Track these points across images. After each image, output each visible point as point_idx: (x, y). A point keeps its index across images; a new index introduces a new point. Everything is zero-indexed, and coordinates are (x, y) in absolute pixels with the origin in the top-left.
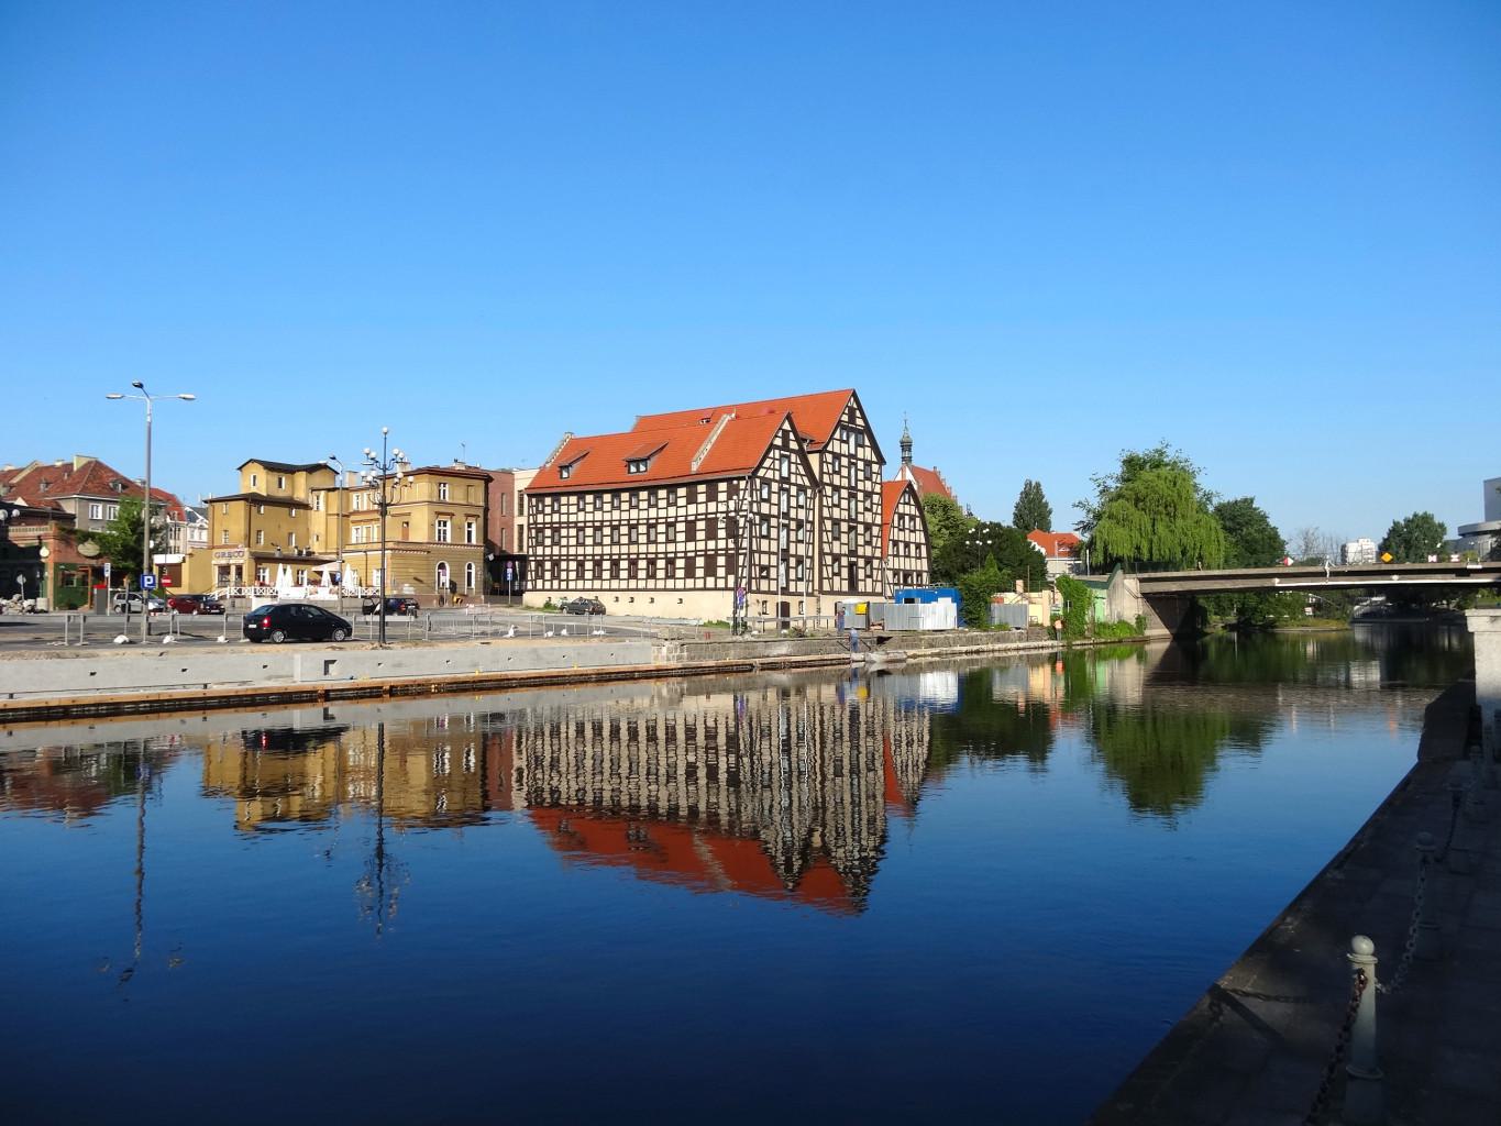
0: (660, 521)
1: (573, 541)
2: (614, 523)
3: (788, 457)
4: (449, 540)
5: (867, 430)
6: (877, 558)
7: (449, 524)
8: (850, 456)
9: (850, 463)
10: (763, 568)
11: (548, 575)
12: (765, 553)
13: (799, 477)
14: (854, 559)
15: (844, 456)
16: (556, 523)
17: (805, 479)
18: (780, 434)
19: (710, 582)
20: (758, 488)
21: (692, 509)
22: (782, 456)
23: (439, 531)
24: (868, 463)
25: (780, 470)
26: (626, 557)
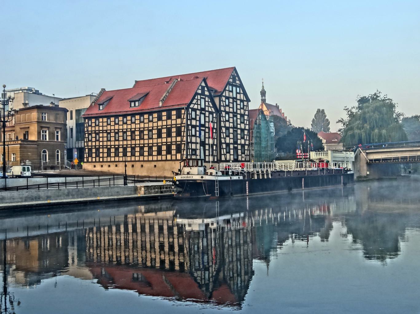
0: (145, 129)
1: (105, 139)
2: (124, 130)
3: (205, 99)
4: (47, 139)
5: (241, 86)
6: (247, 145)
7: (47, 132)
8: (233, 98)
9: (233, 101)
10: (193, 150)
11: (94, 155)
12: (194, 143)
13: (210, 108)
14: (236, 146)
15: (231, 98)
16: (97, 131)
17: (213, 109)
18: (200, 88)
19: (169, 157)
20: (190, 113)
21: (160, 123)
22: (201, 98)
23: (43, 135)
24: (242, 101)
25: (200, 105)
26: (130, 146)
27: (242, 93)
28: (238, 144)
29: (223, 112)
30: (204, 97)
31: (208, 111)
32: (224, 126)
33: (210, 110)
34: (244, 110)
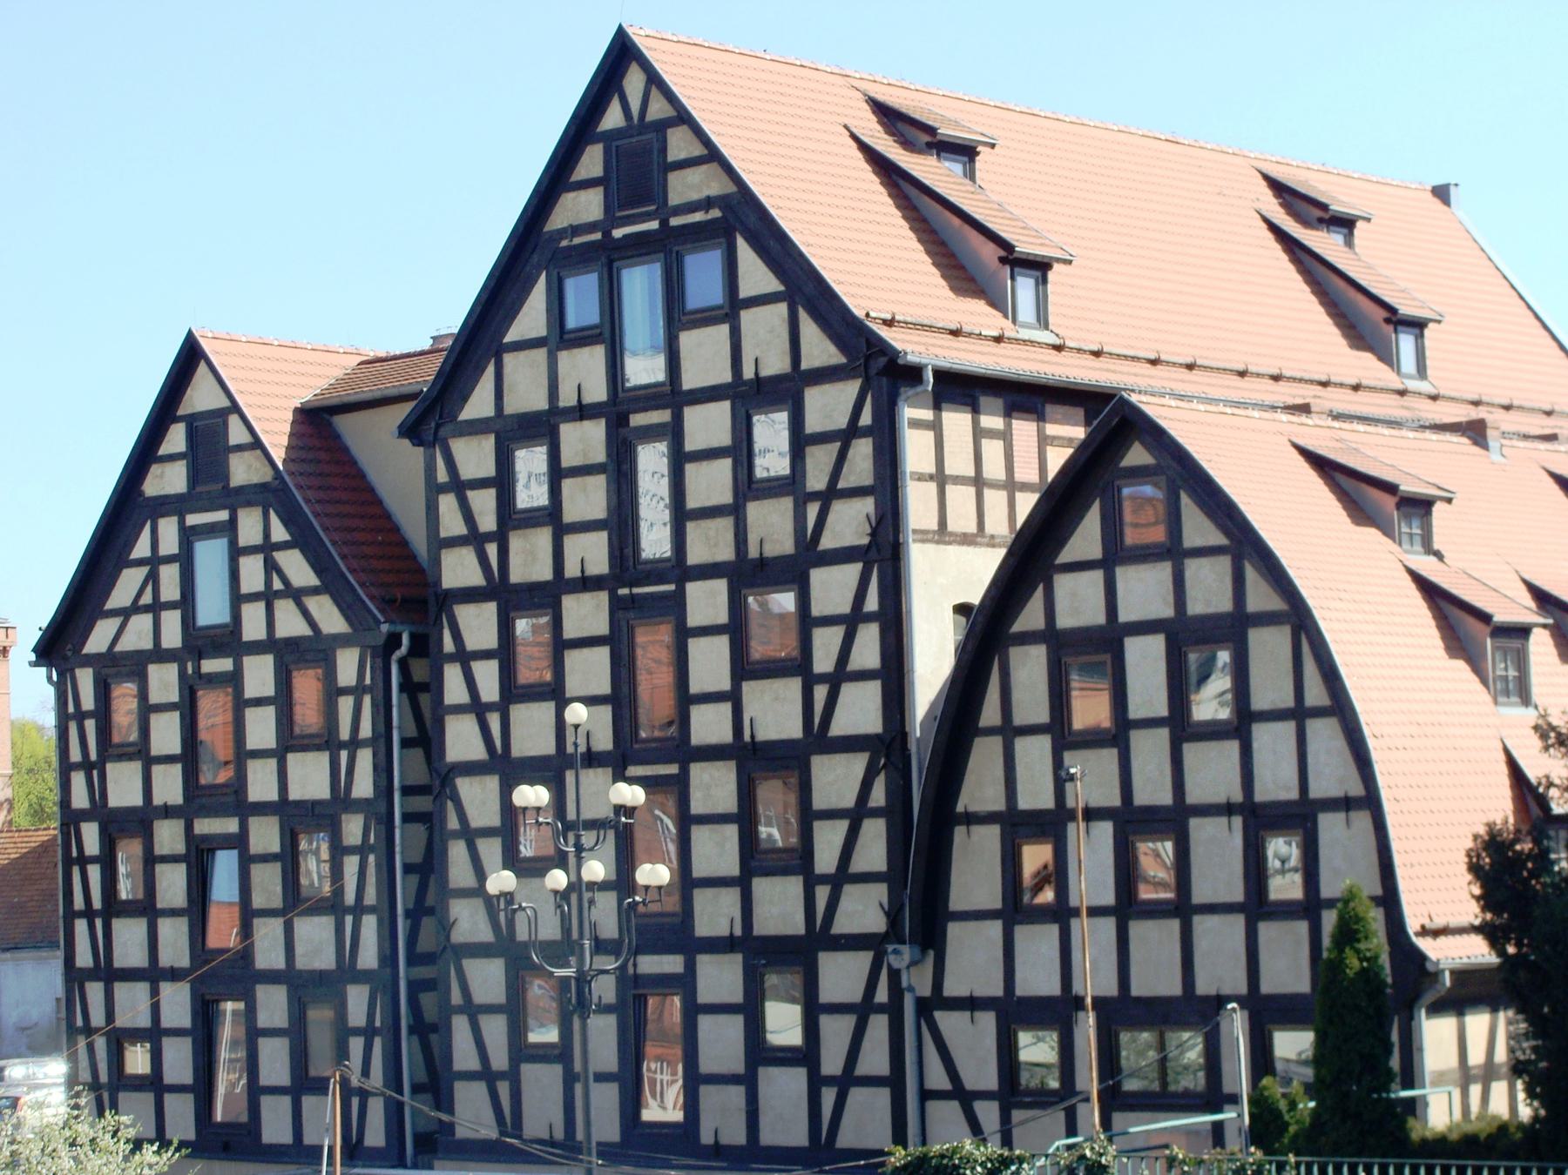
3: (231, 527)
5: (742, 218)
8: (617, 408)
12: (130, 975)
18: (176, 439)
20: (88, 703)
22: (188, 536)
27: (771, 284)
30: (223, 515)
31: (271, 644)
33: (290, 624)
34: (803, 499)
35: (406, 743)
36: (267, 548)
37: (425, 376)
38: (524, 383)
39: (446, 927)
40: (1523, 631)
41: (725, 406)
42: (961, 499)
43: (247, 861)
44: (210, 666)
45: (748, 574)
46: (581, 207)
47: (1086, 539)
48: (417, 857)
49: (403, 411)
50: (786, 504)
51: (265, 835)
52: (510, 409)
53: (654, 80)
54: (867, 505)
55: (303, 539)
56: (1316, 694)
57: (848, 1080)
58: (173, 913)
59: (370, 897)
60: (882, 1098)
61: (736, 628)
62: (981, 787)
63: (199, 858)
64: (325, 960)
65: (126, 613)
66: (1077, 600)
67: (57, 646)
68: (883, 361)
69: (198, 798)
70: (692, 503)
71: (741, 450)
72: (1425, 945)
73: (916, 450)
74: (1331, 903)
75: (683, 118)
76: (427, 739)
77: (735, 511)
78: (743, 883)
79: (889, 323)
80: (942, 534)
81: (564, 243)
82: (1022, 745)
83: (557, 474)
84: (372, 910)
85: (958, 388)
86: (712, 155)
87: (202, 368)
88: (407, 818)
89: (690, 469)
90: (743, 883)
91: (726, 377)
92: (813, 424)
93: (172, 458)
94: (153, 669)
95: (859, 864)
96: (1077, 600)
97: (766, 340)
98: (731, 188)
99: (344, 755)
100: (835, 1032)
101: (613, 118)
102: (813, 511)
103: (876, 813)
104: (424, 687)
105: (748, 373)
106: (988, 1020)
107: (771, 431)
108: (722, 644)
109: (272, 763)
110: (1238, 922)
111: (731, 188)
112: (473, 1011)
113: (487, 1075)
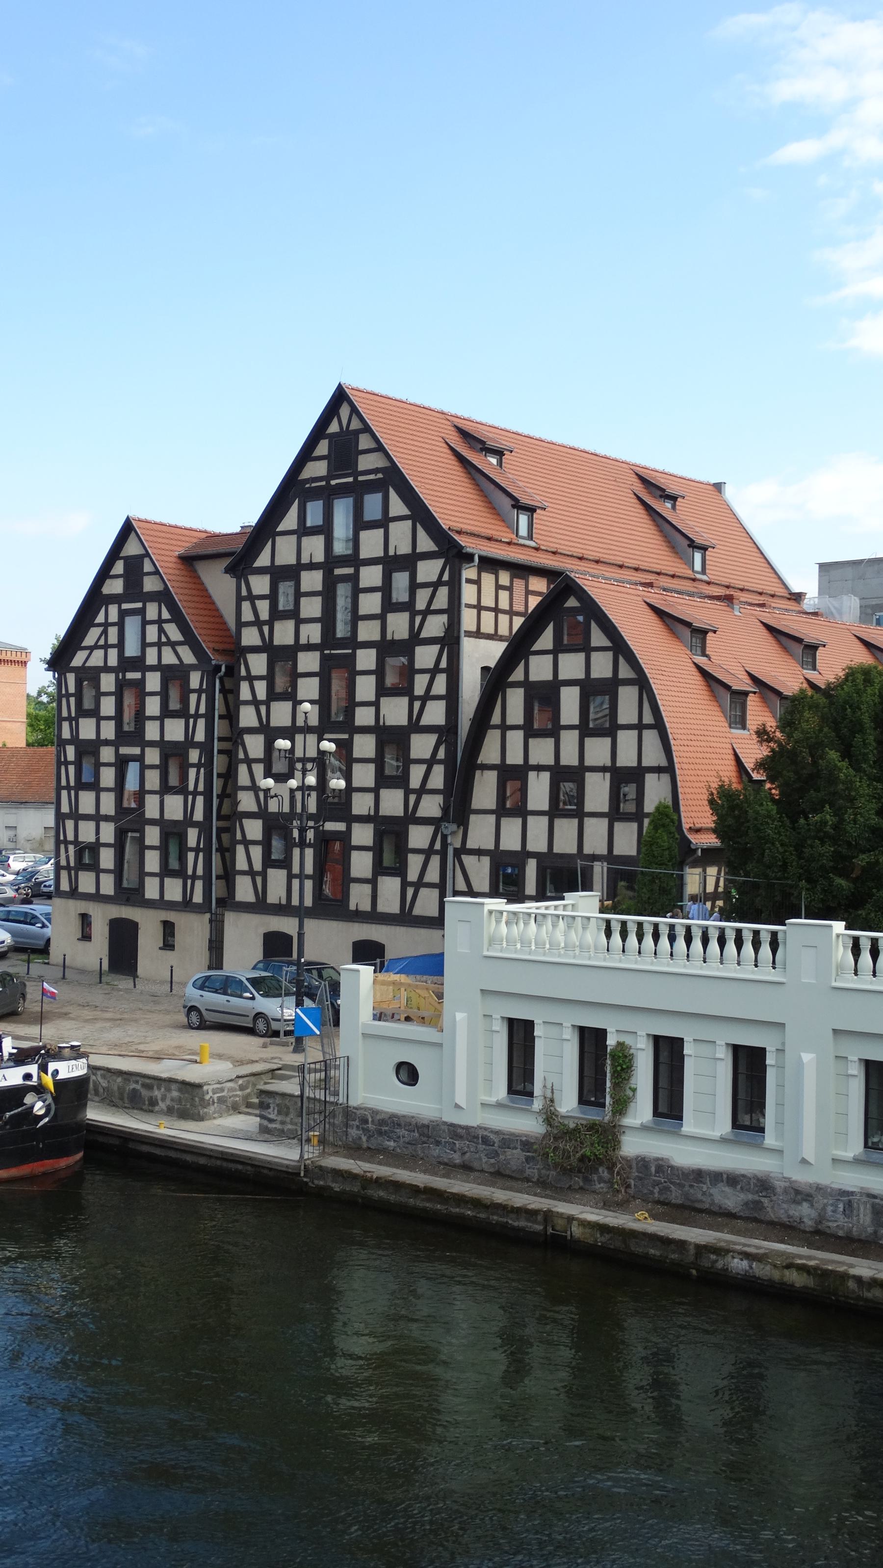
3: (142, 612)
5: (393, 478)
12: (87, 817)
13: (167, 652)
18: (119, 568)
20: (72, 689)
22: (123, 614)
27: (405, 511)
28: (351, 819)
29: (252, 658)
30: (139, 605)
31: (158, 667)
32: (255, 723)
33: (169, 658)
34: (413, 614)
35: (220, 717)
36: (160, 622)
37: (238, 546)
38: (285, 551)
39: (236, 803)
40: (746, 694)
41: (380, 568)
42: (488, 618)
43: (143, 768)
44: (130, 675)
45: (386, 648)
46: (317, 469)
47: (546, 640)
48: (223, 770)
49: (226, 562)
50: (406, 616)
51: (153, 756)
52: (278, 562)
53: (354, 410)
54: (444, 618)
55: (178, 618)
56: (648, 719)
57: (420, 884)
58: (108, 790)
59: (201, 788)
60: (436, 892)
61: (379, 672)
62: (490, 753)
63: (121, 765)
64: (178, 815)
65: (92, 649)
66: (540, 668)
67: (59, 661)
68: (455, 551)
69: (122, 738)
70: (362, 612)
71: (386, 588)
72: (690, 837)
73: (468, 594)
74: (648, 815)
75: (367, 429)
76: (231, 716)
77: (382, 617)
78: (376, 791)
79: (459, 532)
80: (478, 634)
81: (307, 486)
82: (510, 734)
83: (298, 595)
84: (200, 794)
85: (490, 564)
86: (380, 448)
87: (133, 535)
88: (219, 752)
89: (362, 596)
90: (376, 791)
91: (381, 554)
92: (420, 579)
93: (117, 576)
94: (102, 675)
95: (430, 785)
96: (540, 668)
97: (401, 537)
98: (387, 464)
99: (191, 721)
100: (414, 863)
101: (334, 428)
102: (418, 619)
103: (440, 762)
104: (231, 691)
105: (391, 552)
106: (486, 861)
107: (401, 580)
108: (372, 679)
109: (158, 723)
110: (605, 822)
111: (387, 464)
112: (246, 843)
113: (251, 873)
